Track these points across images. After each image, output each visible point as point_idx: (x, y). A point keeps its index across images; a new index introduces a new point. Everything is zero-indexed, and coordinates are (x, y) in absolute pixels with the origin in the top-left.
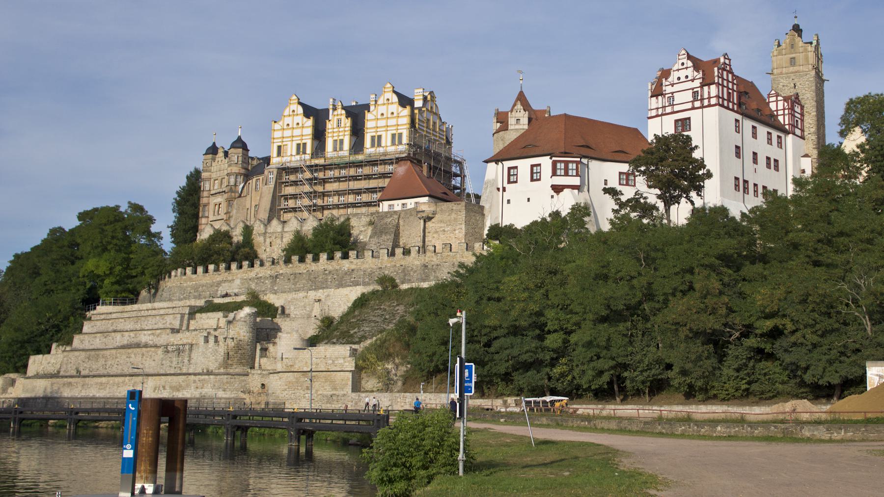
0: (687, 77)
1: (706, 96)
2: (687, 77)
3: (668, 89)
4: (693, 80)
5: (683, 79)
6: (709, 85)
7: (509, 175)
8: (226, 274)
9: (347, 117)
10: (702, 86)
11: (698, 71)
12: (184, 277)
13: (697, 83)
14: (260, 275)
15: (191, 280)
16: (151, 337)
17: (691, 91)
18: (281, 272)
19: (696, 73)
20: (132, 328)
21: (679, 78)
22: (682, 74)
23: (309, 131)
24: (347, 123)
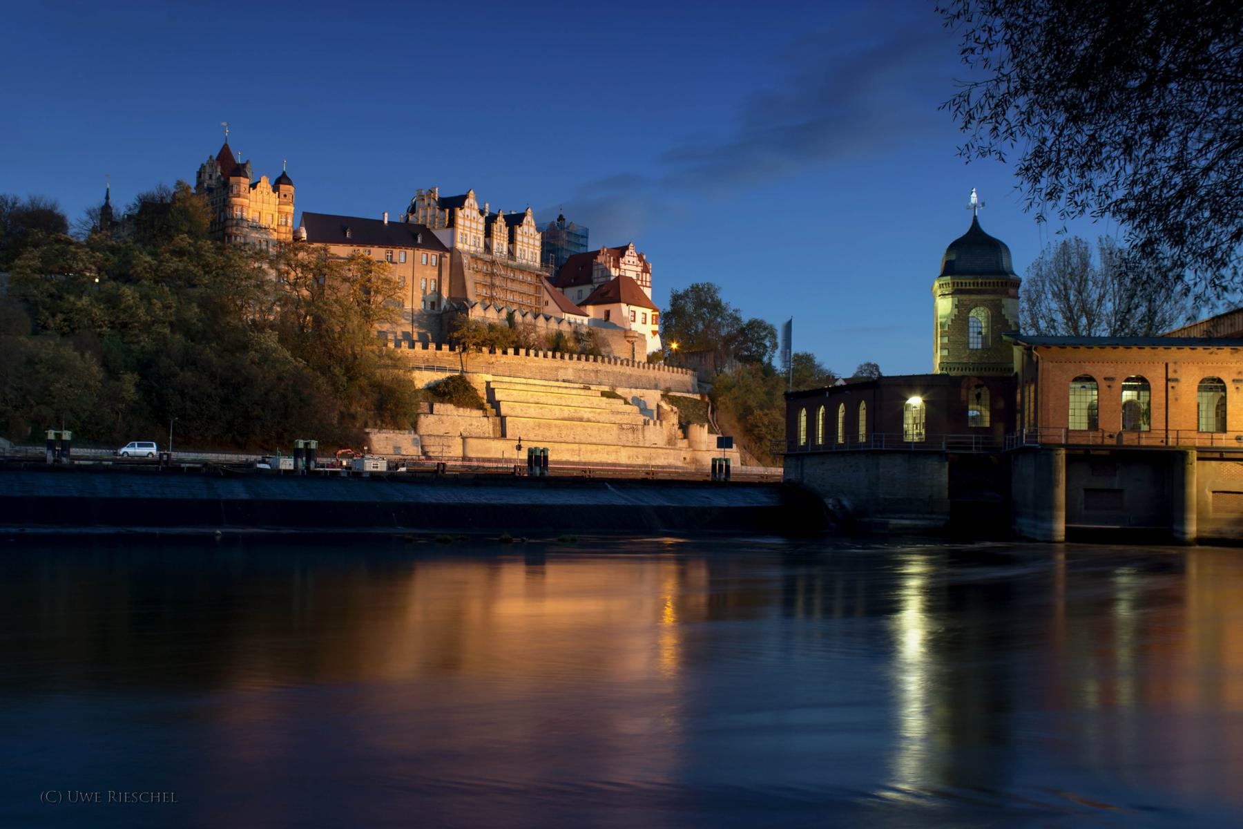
0: (633, 262)
1: (644, 279)
2: (633, 262)
3: (623, 266)
4: (637, 266)
5: (631, 263)
6: (646, 273)
7: (634, 316)
8: (561, 362)
9: (506, 226)
10: (643, 272)
11: (641, 262)
12: (528, 358)
13: (639, 269)
14: (585, 368)
15: (535, 362)
16: (592, 415)
17: (635, 273)
18: (599, 368)
19: (639, 262)
20: (556, 403)
21: (629, 261)
22: (632, 259)
23: (482, 227)
24: (506, 231)
